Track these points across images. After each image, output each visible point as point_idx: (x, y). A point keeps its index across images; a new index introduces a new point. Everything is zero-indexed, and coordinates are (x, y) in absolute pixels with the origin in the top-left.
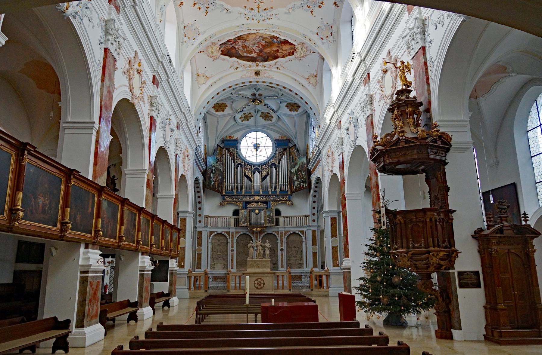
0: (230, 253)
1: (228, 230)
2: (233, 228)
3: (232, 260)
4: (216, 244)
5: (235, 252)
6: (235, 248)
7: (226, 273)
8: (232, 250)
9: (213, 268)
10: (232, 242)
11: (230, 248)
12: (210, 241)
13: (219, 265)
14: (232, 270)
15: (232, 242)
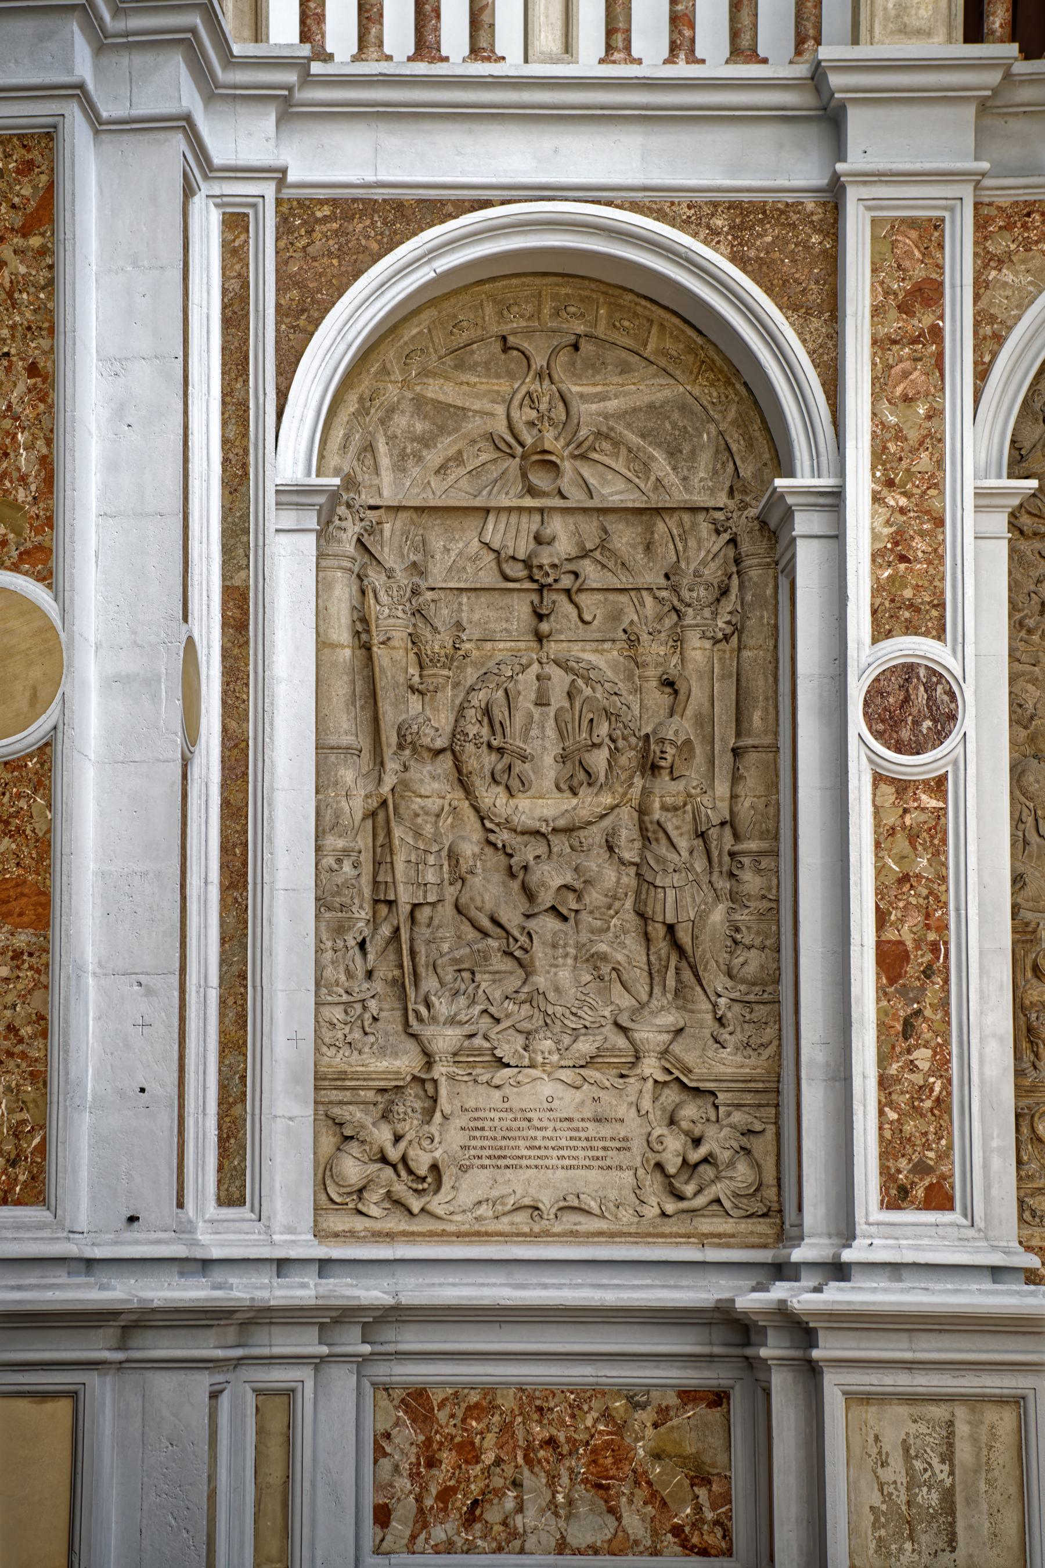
0: (843, 788)
1: (779, 167)
2: (909, 91)
3: (916, 967)
4: (456, 555)
5: (980, 751)
6: (976, 652)
7: (737, 1328)
8: (915, 709)
9: (383, 1154)
10: (910, 467)
11: (840, 628)
12: (290, 454)
13: (546, 1094)
14: (885, 1233)
15: (910, 467)
